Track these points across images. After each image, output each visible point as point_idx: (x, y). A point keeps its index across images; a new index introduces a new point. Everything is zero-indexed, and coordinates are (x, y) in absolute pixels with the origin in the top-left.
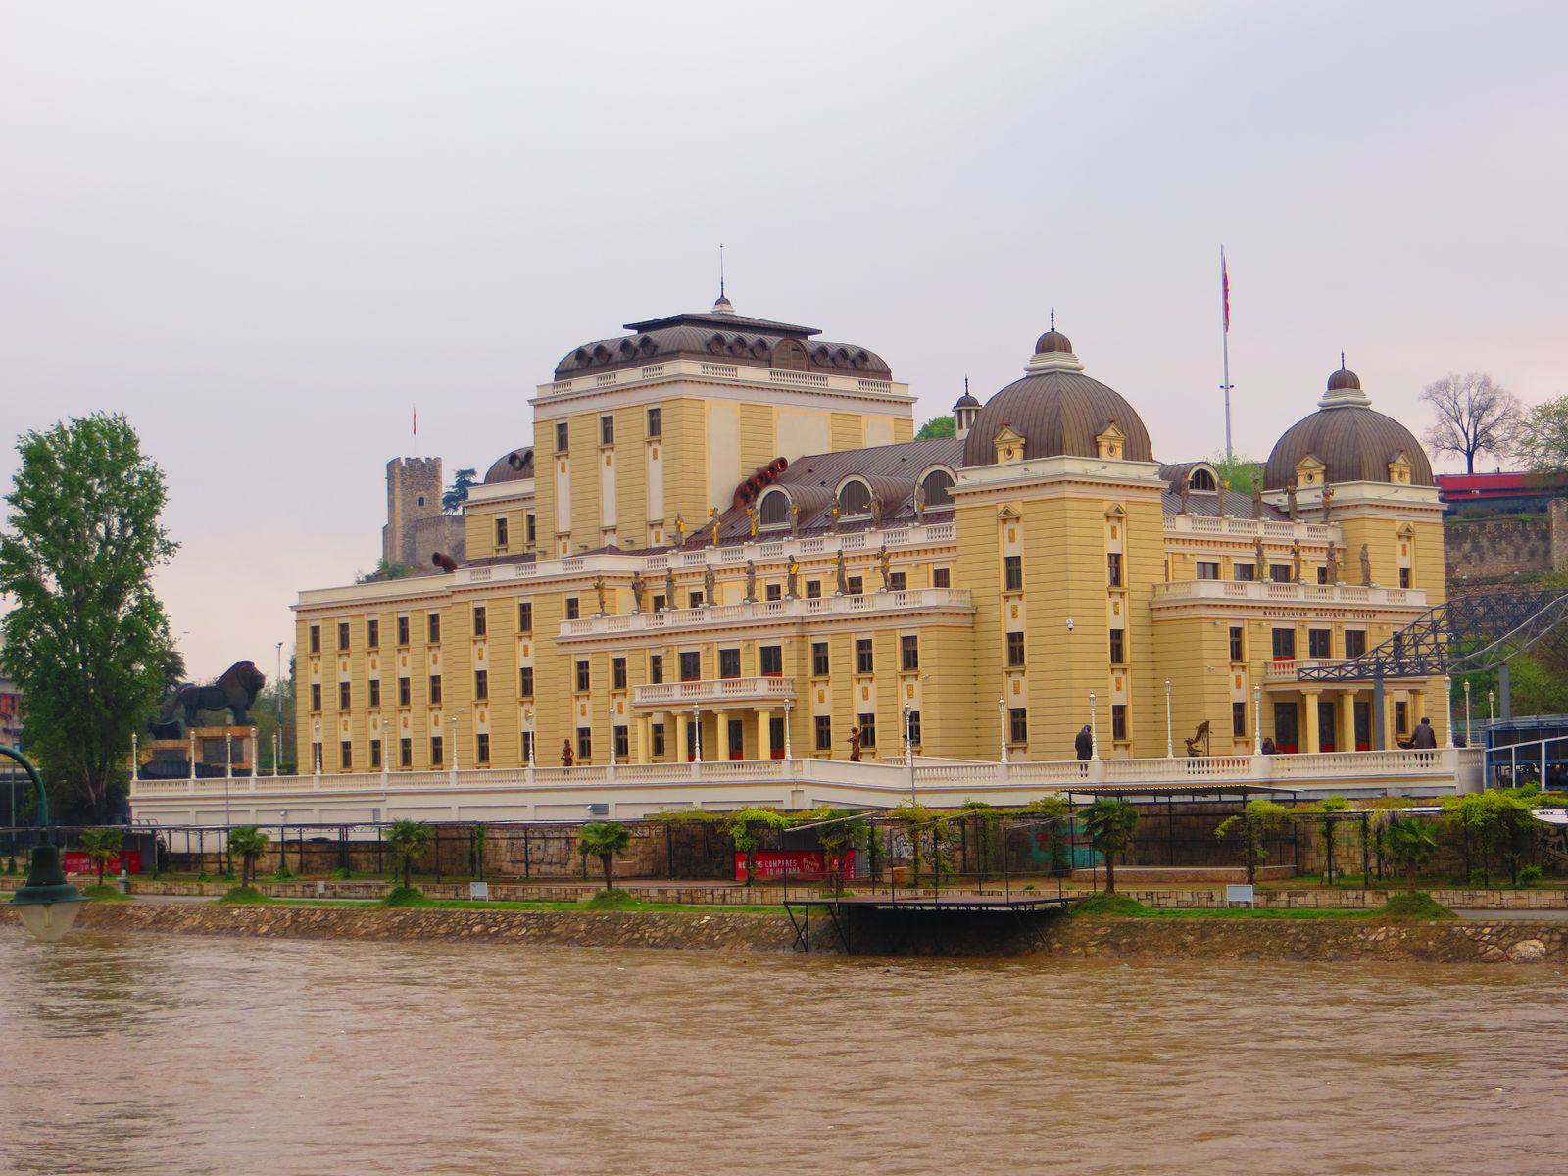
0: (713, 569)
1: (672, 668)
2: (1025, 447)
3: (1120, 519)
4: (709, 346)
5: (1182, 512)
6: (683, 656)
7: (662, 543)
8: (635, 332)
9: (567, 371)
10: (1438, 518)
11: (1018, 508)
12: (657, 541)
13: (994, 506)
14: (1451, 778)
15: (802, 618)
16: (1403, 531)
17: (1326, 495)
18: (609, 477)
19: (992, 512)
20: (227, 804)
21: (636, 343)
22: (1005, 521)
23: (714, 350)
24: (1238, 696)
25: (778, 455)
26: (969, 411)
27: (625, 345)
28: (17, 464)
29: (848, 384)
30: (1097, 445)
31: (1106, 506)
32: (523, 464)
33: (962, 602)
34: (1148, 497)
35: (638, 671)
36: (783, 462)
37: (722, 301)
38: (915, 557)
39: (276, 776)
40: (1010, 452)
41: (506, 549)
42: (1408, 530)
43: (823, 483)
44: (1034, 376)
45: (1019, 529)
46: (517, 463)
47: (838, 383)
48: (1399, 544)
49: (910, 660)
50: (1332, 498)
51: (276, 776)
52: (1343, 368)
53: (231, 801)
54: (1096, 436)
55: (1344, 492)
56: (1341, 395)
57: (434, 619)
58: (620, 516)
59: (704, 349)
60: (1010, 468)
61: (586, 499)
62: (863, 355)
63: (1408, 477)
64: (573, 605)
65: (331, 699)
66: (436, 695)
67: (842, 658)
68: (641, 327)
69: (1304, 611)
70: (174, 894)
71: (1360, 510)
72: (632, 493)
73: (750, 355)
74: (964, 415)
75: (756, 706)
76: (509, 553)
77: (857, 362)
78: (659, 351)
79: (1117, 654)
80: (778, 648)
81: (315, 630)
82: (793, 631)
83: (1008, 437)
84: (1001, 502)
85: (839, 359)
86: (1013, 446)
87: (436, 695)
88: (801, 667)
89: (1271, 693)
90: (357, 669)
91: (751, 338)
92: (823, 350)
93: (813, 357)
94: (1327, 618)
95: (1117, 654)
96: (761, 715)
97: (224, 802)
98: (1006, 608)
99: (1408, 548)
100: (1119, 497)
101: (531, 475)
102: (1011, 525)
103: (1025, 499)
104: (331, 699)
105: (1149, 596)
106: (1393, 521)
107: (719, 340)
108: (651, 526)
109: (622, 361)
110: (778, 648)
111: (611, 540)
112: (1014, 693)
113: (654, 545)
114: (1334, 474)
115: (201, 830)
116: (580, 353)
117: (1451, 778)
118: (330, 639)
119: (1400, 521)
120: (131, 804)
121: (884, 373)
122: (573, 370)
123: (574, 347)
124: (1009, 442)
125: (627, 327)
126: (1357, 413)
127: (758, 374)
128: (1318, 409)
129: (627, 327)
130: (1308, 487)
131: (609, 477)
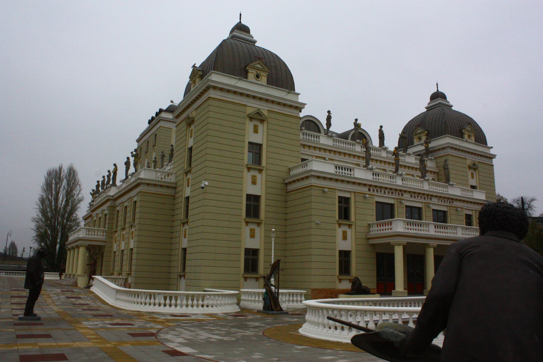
3: (262, 121)
16: (471, 164)
24: (345, 246)
30: (247, 72)
31: (249, 111)
42: (474, 165)
52: (438, 90)
54: (246, 67)
63: (473, 138)
69: (402, 192)
71: (445, 151)
89: (373, 245)
94: (419, 199)
99: (475, 175)
100: (264, 108)
114: (431, 135)
128: (425, 110)
130: (419, 143)
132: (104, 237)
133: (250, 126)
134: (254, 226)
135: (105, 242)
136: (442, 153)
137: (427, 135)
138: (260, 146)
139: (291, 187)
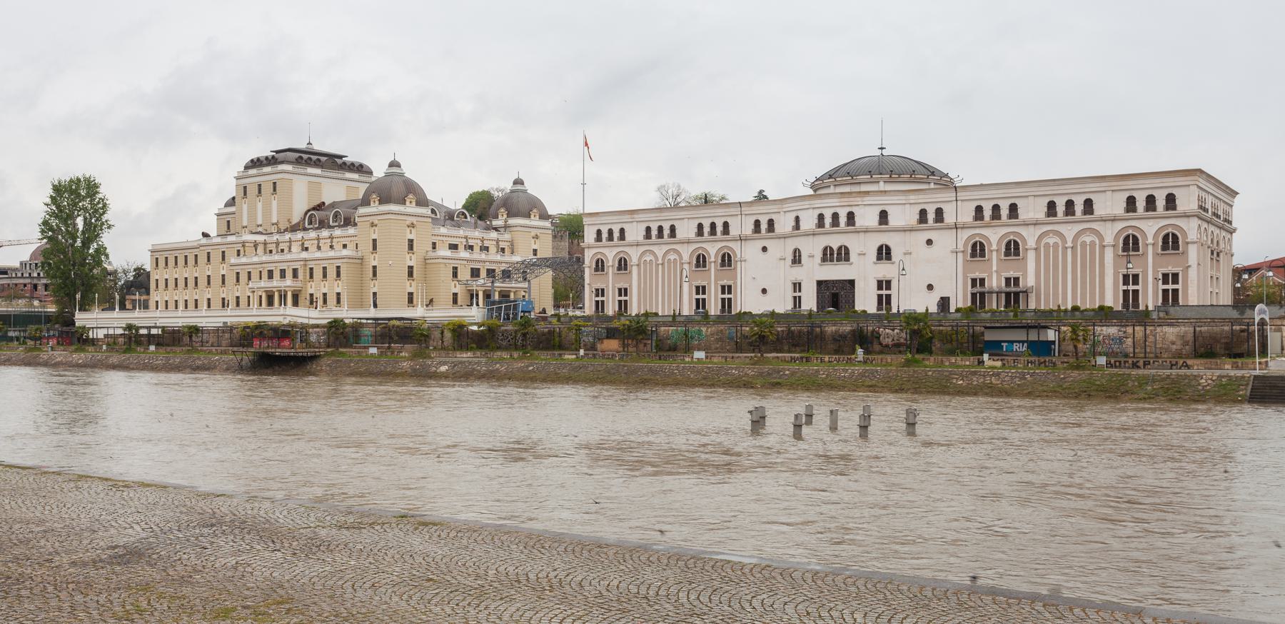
1: (265, 275)
2: (379, 200)
3: (413, 227)
4: (296, 160)
5: (444, 226)
6: (269, 271)
10: (550, 232)
11: (376, 222)
14: (474, 317)
17: (506, 222)
18: (260, 205)
19: (368, 223)
21: (270, 158)
23: (299, 161)
27: (267, 158)
28: (50, 192)
29: (355, 176)
30: (405, 201)
31: (408, 223)
33: (360, 254)
34: (425, 220)
35: (255, 276)
36: (324, 203)
37: (309, 143)
40: (374, 202)
45: (376, 229)
47: (349, 175)
48: (533, 240)
49: (338, 275)
55: (512, 221)
57: (196, 256)
58: (263, 220)
60: (375, 208)
62: (361, 166)
64: (239, 251)
65: (162, 284)
66: (196, 284)
67: (318, 273)
68: (277, 152)
69: (485, 262)
72: (267, 212)
78: (278, 161)
79: (411, 274)
81: (157, 259)
82: (302, 263)
83: (374, 196)
85: (352, 167)
87: (196, 284)
88: (305, 276)
90: (170, 274)
91: (314, 158)
92: (344, 163)
93: (340, 165)
95: (411, 274)
100: (414, 220)
102: (374, 228)
104: (162, 284)
105: (425, 255)
107: (301, 157)
108: (273, 224)
111: (260, 229)
112: (374, 287)
114: (510, 215)
116: (252, 161)
117: (474, 317)
118: (162, 263)
119: (534, 232)
123: (250, 159)
126: (521, 194)
127: (318, 171)
131: (260, 205)
133: (408, 230)
134: (411, 281)
137: (507, 214)
138: (413, 240)
139: (428, 261)
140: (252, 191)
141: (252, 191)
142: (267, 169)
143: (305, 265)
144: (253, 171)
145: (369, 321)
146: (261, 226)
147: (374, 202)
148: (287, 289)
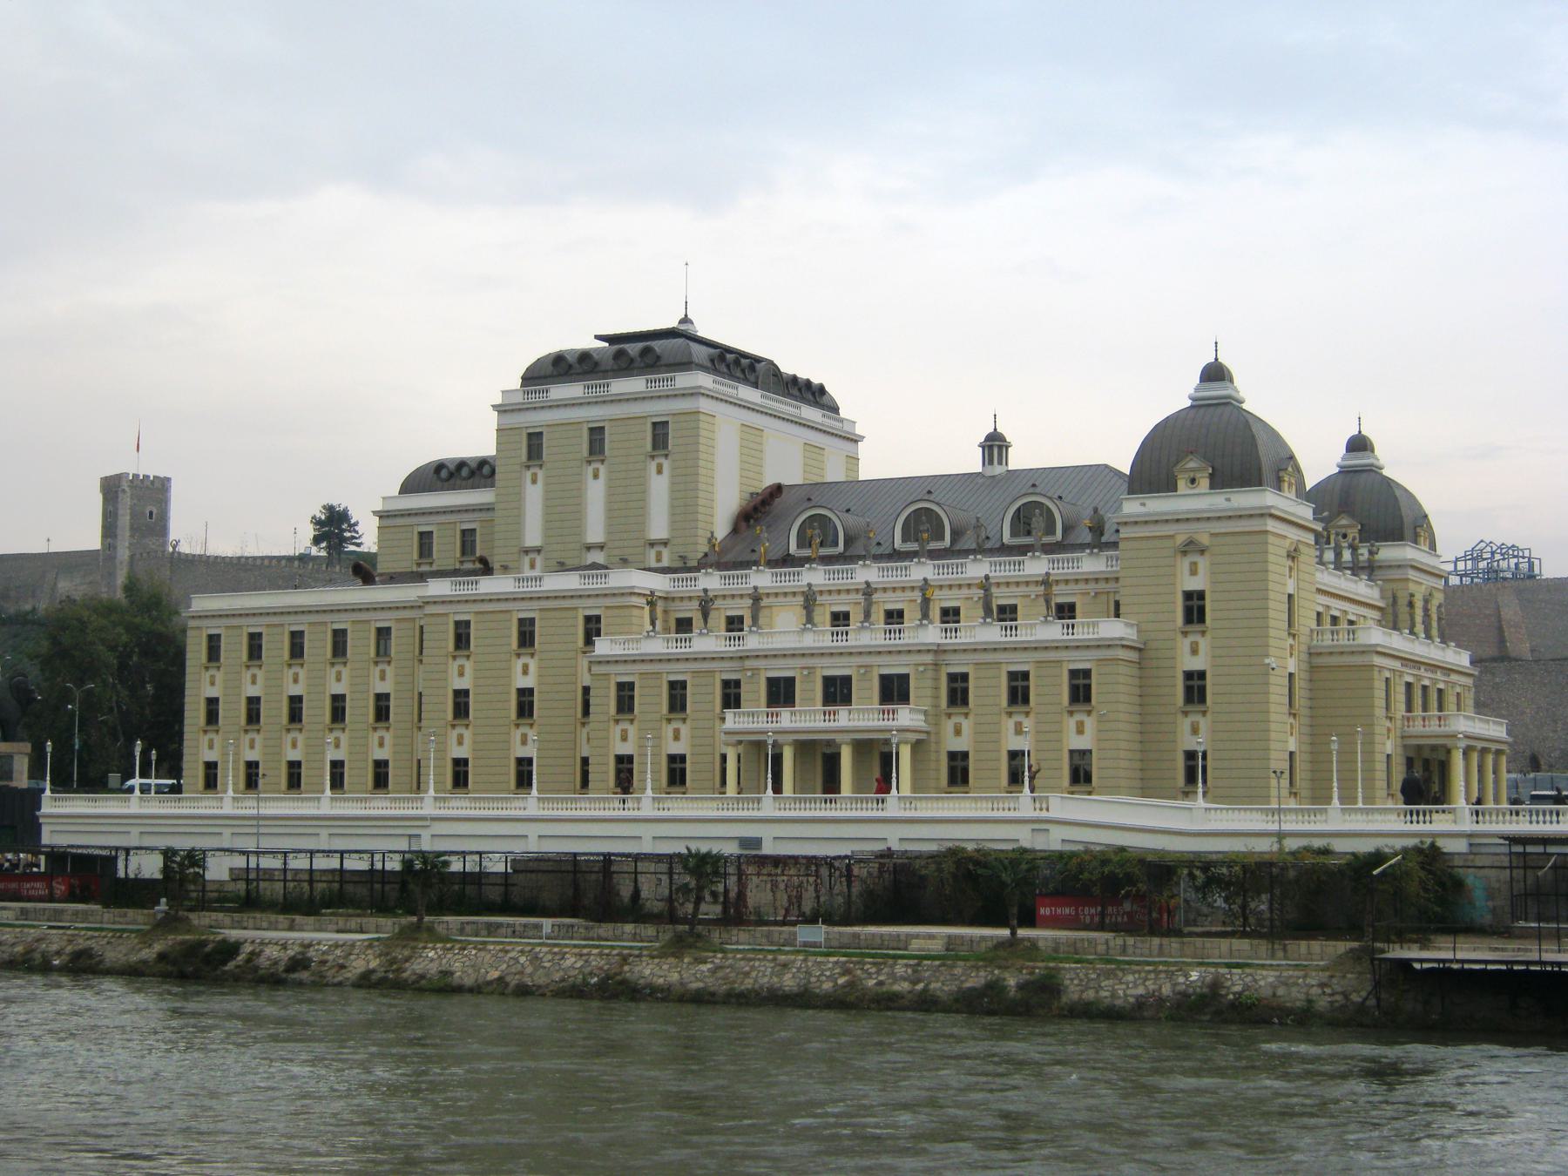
0: (815, 589)
2: (1212, 476)
7: (665, 563)
8: (607, 345)
9: (539, 378)
11: (1205, 540)
12: (659, 560)
13: (1171, 537)
15: (939, 645)
18: (595, 493)
19: (1168, 543)
20: (258, 826)
22: (1184, 553)
25: (769, 481)
26: (1000, 447)
32: (451, 475)
37: (685, 320)
38: (1091, 586)
39: (153, 794)
40: (1193, 481)
41: (431, 564)
43: (848, 511)
44: (1198, 405)
45: (1203, 563)
46: (444, 474)
50: (1377, 557)
51: (153, 794)
53: (261, 823)
56: (1362, 458)
59: (709, 365)
61: (563, 512)
62: (821, 390)
63: (1427, 543)
70: (245, 928)
73: (742, 376)
74: (996, 451)
75: (838, 737)
76: (434, 568)
77: (813, 393)
80: (907, 676)
82: (929, 658)
83: (1192, 465)
84: (1182, 534)
86: (1198, 475)
96: (16, 758)
97: (255, 822)
98: (1184, 644)
101: (493, 486)
103: (1213, 531)
106: (1421, 584)
109: (613, 370)
110: (907, 676)
112: (1194, 734)
113: (654, 564)
115: (285, 853)
120: (41, 820)
121: (835, 409)
122: (545, 377)
124: (1192, 470)
125: (599, 337)
128: (1337, 470)
129: (599, 337)
131: (595, 493)
132: (923, 724)
135: (928, 733)
136: (1396, 574)
140: (565, 449)
141: (565, 449)
142: (574, 390)
143: (936, 666)
144: (560, 392)
145: (1530, 849)
146: (601, 547)
147: (1193, 481)
148: (780, 738)
